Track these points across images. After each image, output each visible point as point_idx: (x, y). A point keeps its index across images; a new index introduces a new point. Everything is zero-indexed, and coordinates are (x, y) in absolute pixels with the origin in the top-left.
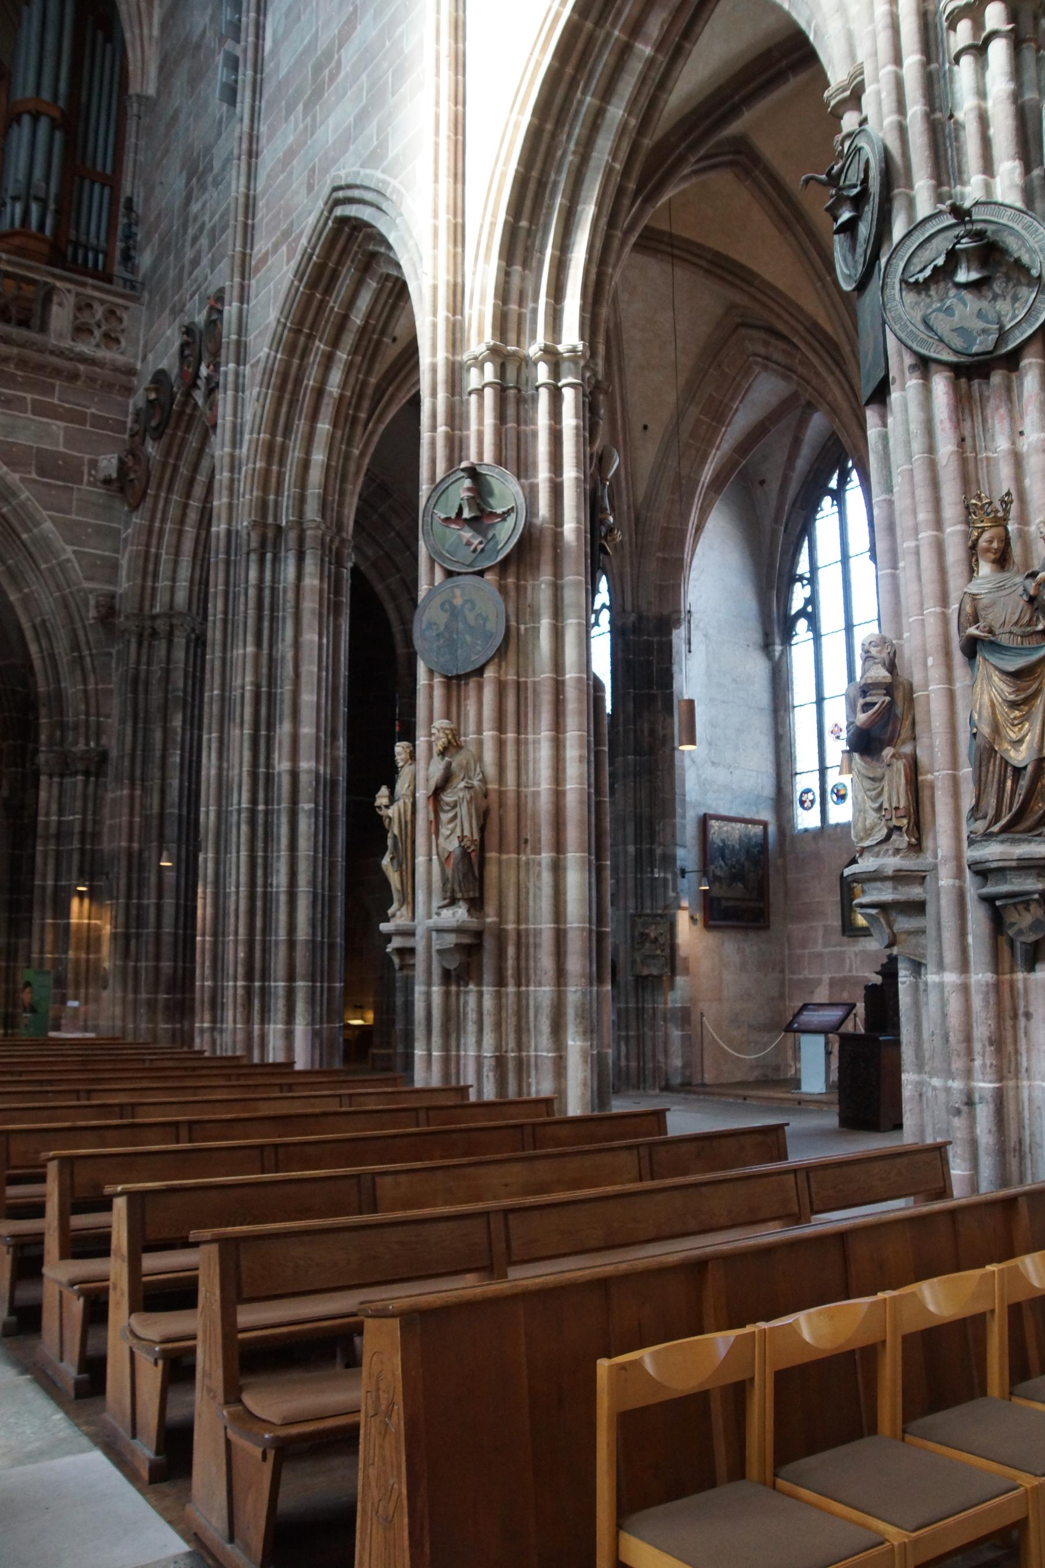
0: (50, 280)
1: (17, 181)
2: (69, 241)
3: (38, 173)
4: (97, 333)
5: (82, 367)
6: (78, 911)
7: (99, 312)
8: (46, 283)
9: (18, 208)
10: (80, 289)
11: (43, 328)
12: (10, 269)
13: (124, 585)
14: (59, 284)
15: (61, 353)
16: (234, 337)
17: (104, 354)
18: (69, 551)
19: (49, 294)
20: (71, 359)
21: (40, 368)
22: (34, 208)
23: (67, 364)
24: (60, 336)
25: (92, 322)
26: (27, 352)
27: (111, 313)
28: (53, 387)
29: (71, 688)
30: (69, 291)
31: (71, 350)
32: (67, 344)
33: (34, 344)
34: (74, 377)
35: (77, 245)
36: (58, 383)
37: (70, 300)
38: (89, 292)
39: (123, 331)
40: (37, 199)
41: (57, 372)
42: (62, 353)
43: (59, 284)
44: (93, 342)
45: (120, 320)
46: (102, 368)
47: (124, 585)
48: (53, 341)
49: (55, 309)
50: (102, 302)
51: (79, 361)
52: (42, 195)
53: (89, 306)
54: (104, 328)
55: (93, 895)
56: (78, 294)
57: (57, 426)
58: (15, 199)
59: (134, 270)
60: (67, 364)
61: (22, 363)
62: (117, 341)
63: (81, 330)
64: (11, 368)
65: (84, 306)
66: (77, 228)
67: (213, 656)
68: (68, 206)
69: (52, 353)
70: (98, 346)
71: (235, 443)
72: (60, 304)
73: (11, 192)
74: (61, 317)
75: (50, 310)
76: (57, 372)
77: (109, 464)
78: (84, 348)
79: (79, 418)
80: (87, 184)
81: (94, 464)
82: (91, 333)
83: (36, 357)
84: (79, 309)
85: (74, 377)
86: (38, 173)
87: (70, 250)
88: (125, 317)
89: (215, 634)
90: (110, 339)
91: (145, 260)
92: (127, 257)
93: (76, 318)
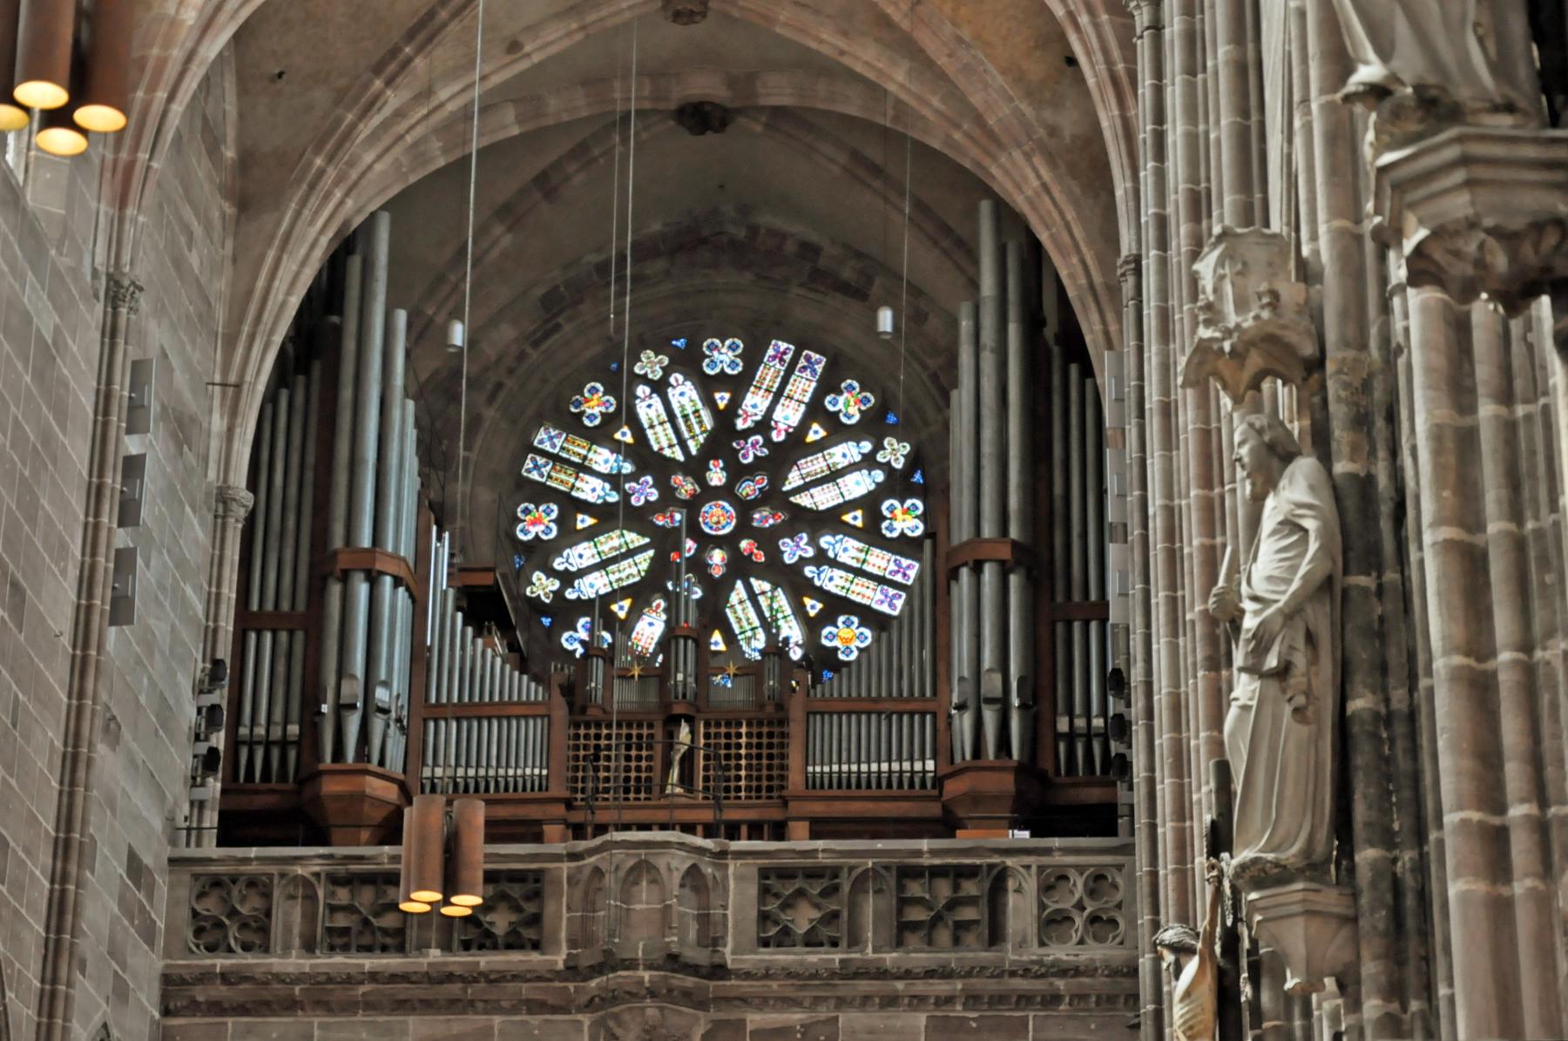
0: (996, 860)
1: (961, 679)
2: (1058, 736)
3: (988, 660)
4: (1079, 921)
5: (1061, 984)
7: (1079, 883)
8: (991, 867)
9: (965, 722)
10: (1045, 860)
11: (996, 936)
12: (937, 861)
14: (1009, 862)
15: (1026, 972)
16: (1150, 1007)
17: (1095, 953)
19: (998, 882)
20: (1043, 976)
21: (999, 999)
22: (990, 717)
23: (1038, 985)
24: (1022, 944)
25: (1067, 904)
26: (978, 983)
28: (1025, 1020)
30: (1028, 867)
31: (1040, 963)
32: (1033, 952)
33: (983, 968)
34: (1053, 999)
35: (1071, 737)
36: (1031, 1015)
37: (1031, 885)
38: (1058, 859)
39: (1119, 906)
40: (990, 701)
41: (1025, 1000)
42: (1027, 970)
43: (1009, 862)
44: (1075, 939)
45: (1115, 886)
46: (1092, 976)
48: (1011, 955)
49: (1012, 899)
50: (1080, 869)
51: (1054, 975)
52: (997, 691)
53: (1064, 878)
54: (1089, 910)
56: (1041, 869)
58: (961, 707)
60: (1038, 985)
61: (972, 999)
62: (1113, 923)
63: (1052, 924)
64: (958, 1010)
65: (1052, 882)
66: (1070, 713)
68: (1042, 689)
69: (1013, 974)
70: (1081, 942)
72: (1018, 891)
73: (955, 700)
74: (1021, 908)
75: (1005, 905)
76: (1025, 1000)
78: (1059, 953)
80: (1077, 626)
82: (1070, 919)
83: (990, 986)
84: (1046, 888)
85: (1053, 999)
86: (988, 660)
87: (1062, 747)
88: (1120, 881)
93: (1042, 907)
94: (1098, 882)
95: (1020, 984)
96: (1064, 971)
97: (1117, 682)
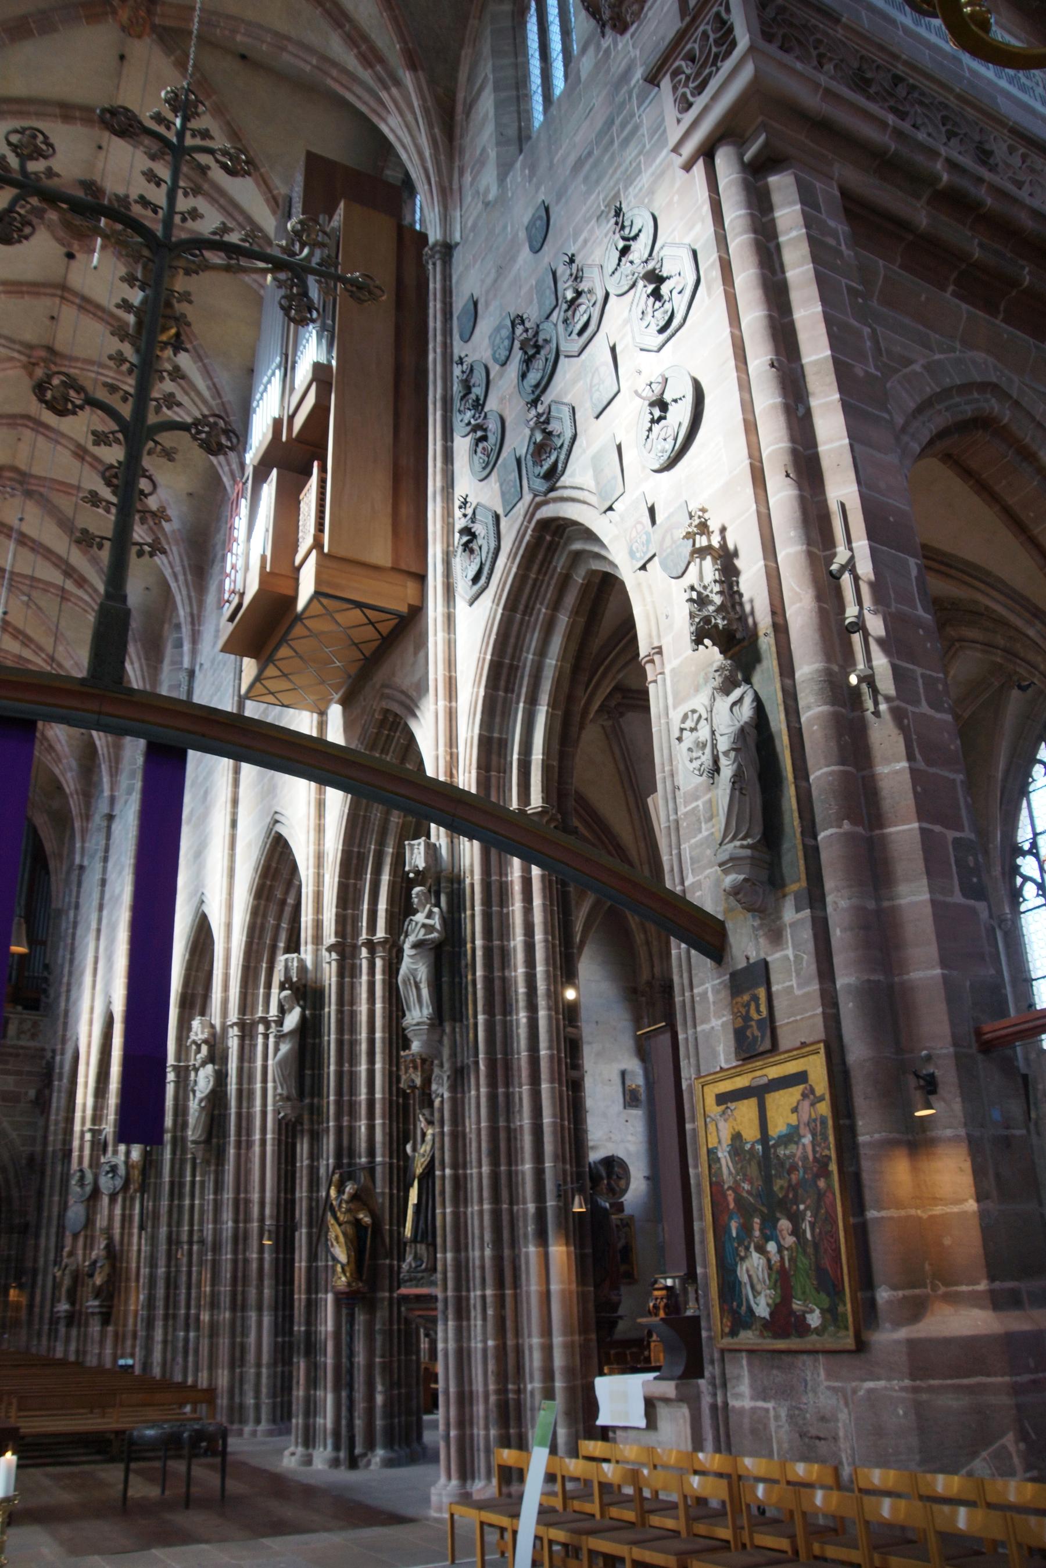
6: (13, 1294)
13: (38, 1149)
15: (12, 1047)
17: (32, 1044)
18: (14, 1135)
27: (35, 1024)
29: (15, 1193)
32: (15, 1042)
34: (17, 1055)
41: (11, 1055)
47: (38, 1149)
48: (9, 1042)
55: (20, 1287)
57: (10, 1079)
59: (48, 997)
63: (20, 1032)
67: (46, 1199)
71: (57, 1115)
76: (11, 1055)
77: (32, 1093)
78: (22, 1043)
79: (18, 1073)
81: (26, 1093)
85: (17, 1055)
89: (47, 1191)
90: (33, 1036)
91: (52, 992)
92: (45, 991)
94: (35, 1024)
95: (11, 1050)
96: (22, 1047)
97: (46, 967)
